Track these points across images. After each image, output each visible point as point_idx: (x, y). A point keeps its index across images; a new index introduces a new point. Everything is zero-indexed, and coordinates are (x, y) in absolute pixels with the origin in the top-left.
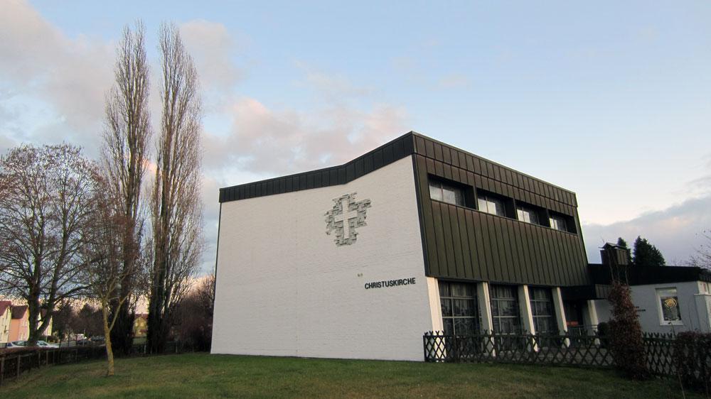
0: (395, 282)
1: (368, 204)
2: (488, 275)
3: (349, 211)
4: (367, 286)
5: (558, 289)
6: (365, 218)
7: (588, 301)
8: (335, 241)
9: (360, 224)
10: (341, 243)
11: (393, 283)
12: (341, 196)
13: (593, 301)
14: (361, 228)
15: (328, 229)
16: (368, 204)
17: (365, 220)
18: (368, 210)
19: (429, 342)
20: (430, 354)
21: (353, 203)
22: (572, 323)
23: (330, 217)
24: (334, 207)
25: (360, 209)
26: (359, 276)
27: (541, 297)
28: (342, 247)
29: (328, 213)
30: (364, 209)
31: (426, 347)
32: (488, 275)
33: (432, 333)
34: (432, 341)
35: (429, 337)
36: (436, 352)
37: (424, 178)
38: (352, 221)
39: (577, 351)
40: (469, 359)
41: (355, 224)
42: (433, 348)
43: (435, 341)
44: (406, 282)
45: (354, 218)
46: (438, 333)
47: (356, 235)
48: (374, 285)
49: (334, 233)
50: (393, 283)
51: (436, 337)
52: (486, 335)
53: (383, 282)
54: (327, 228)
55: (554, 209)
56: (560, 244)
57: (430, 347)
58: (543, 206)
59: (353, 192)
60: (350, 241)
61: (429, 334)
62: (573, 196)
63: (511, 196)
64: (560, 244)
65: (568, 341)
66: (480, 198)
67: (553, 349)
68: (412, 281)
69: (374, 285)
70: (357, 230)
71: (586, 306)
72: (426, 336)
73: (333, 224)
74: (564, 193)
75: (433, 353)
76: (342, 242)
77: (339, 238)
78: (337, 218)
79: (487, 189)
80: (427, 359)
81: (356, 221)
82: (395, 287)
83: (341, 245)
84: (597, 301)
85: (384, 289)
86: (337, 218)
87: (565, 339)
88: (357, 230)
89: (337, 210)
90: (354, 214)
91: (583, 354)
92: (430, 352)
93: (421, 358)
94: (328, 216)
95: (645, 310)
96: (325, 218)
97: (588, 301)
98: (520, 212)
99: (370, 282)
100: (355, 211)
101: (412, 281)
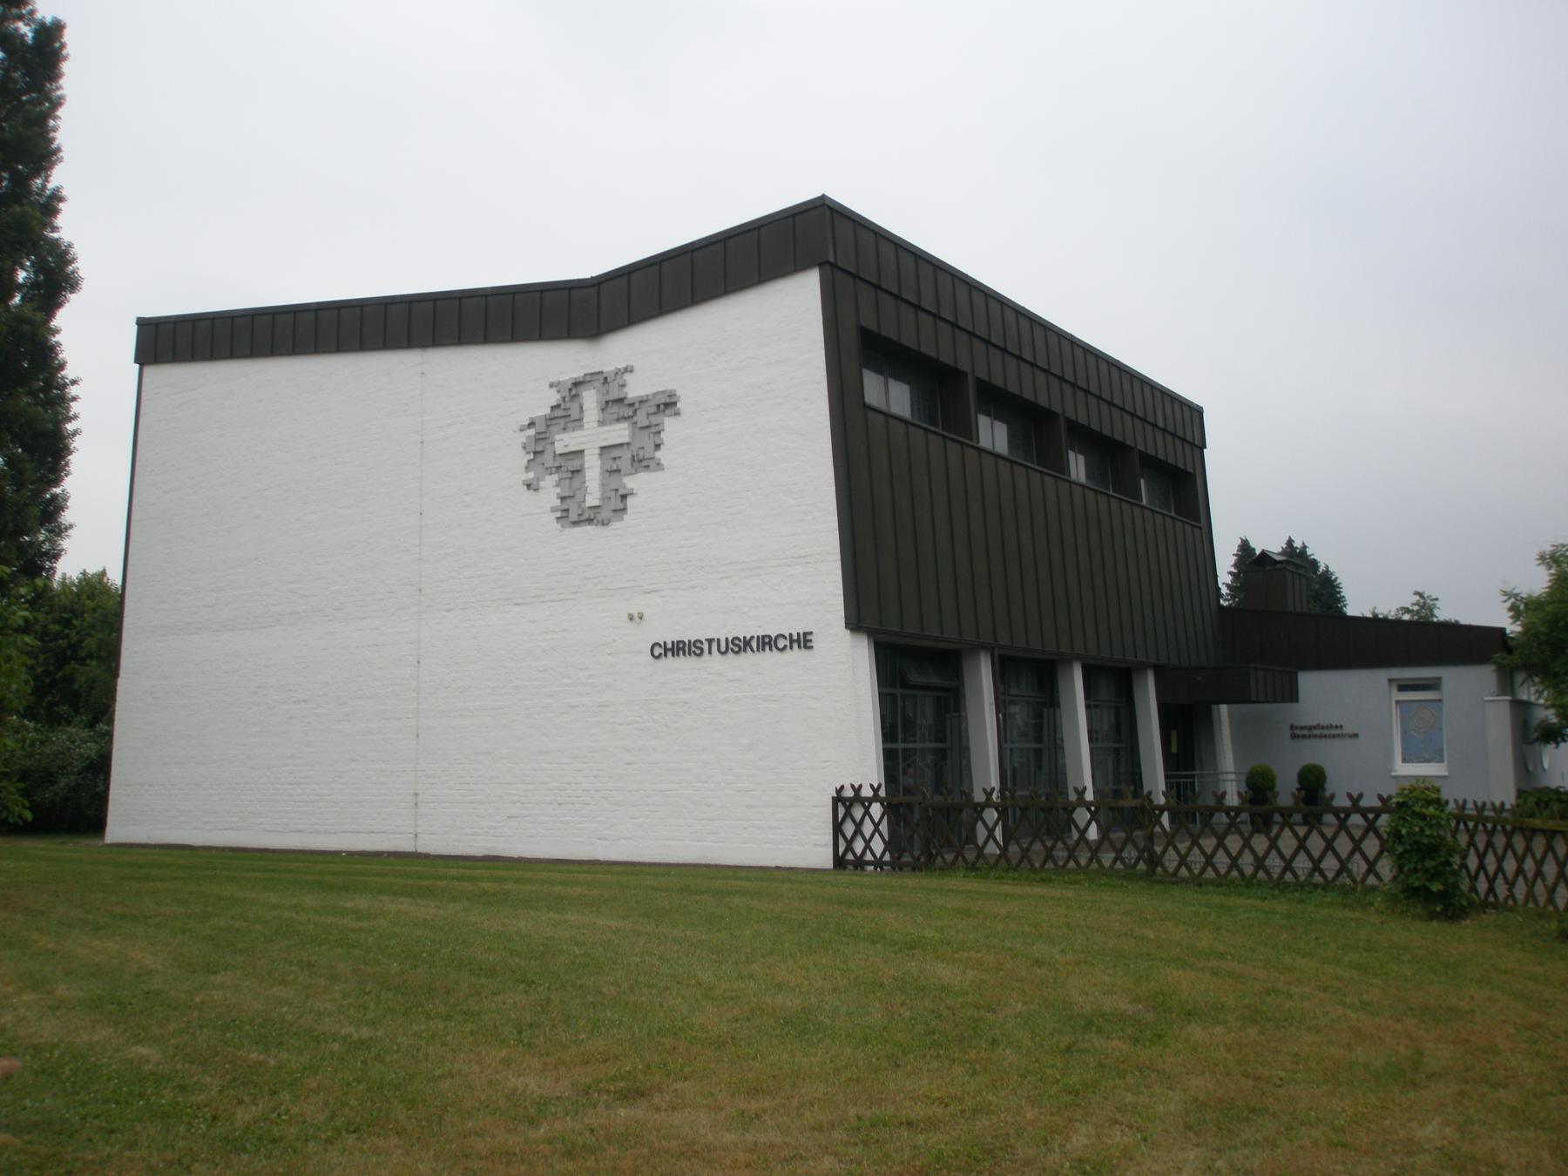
0: (747, 643)
1: (668, 404)
2: (995, 631)
3: (602, 423)
4: (657, 651)
5: (1151, 680)
6: (658, 447)
7: (1214, 707)
8: (553, 510)
9: (642, 463)
10: (573, 516)
11: (740, 646)
12: (578, 374)
13: (1224, 708)
14: (643, 477)
15: (531, 475)
16: (668, 404)
17: (658, 454)
18: (670, 424)
19: (848, 814)
20: (849, 848)
21: (620, 401)
22: (1170, 773)
23: (541, 438)
24: (553, 408)
25: (641, 419)
26: (631, 618)
27: (1105, 691)
28: (578, 530)
29: (532, 424)
30: (654, 420)
31: (838, 828)
32: (995, 631)
33: (857, 790)
34: (858, 812)
35: (845, 803)
36: (868, 843)
37: (851, 339)
38: (615, 453)
39: (1168, 845)
40: (850, 862)
41: (625, 464)
42: (858, 831)
43: (867, 812)
44: (781, 643)
45: (621, 445)
46: (989, 794)
47: (624, 497)
48: (678, 649)
49: (550, 488)
50: (740, 646)
51: (871, 801)
52: (1220, 806)
53: (710, 641)
54: (527, 469)
55: (1151, 452)
56: (1162, 549)
57: (849, 829)
58: (1128, 442)
59: (622, 366)
60: (605, 514)
61: (849, 793)
62: (1196, 415)
63: (1056, 408)
64: (1162, 549)
65: (1165, 819)
66: (980, 413)
67: (1118, 836)
68: (803, 641)
69: (678, 649)
70: (630, 482)
71: (1209, 720)
72: (838, 799)
73: (548, 459)
74: (1186, 410)
75: (859, 846)
76: (573, 514)
77: (569, 504)
78: (565, 441)
79: (1001, 385)
80: (839, 862)
81: (626, 455)
82: (748, 658)
83: (576, 523)
84: (1231, 706)
85: (713, 663)
86: (565, 441)
87: (1161, 813)
88: (630, 482)
89: (564, 414)
90: (620, 433)
91: (1183, 852)
92: (850, 843)
93: (822, 857)
94: (532, 432)
95: (1356, 735)
96: (522, 438)
97: (1214, 707)
98: (983, 422)
99: (670, 638)
100: (624, 425)
101: (803, 641)
